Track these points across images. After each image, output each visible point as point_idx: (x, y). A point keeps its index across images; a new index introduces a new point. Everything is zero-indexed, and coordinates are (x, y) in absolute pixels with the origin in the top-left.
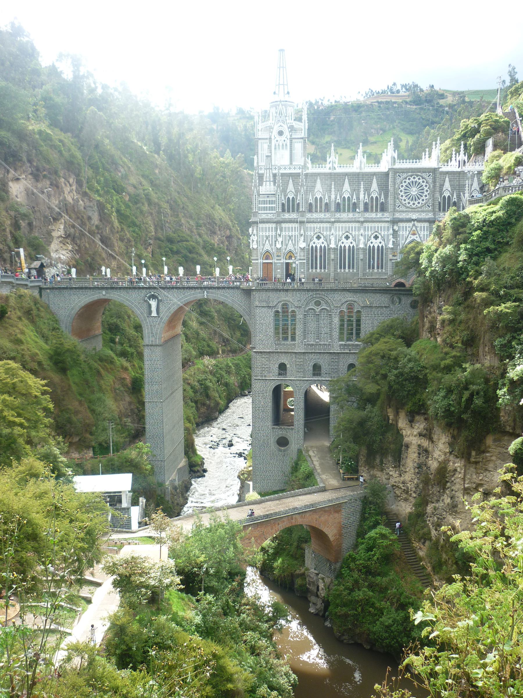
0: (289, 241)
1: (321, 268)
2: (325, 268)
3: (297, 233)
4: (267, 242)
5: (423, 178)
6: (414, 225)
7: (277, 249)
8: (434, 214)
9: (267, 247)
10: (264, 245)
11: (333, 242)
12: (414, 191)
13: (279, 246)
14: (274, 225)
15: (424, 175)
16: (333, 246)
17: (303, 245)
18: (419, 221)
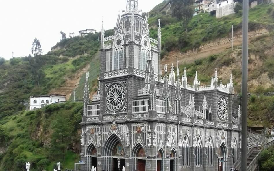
0: (172, 140)
1: (186, 165)
2: (188, 165)
3: (176, 134)
4: (161, 141)
5: (226, 100)
6: (223, 132)
7: (168, 147)
8: (230, 125)
9: (161, 146)
10: (158, 144)
11: (195, 142)
12: (222, 109)
13: (168, 145)
14: (164, 125)
15: (226, 98)
16: (195, 146)
17: (180, 145)
18: (225, 130)
